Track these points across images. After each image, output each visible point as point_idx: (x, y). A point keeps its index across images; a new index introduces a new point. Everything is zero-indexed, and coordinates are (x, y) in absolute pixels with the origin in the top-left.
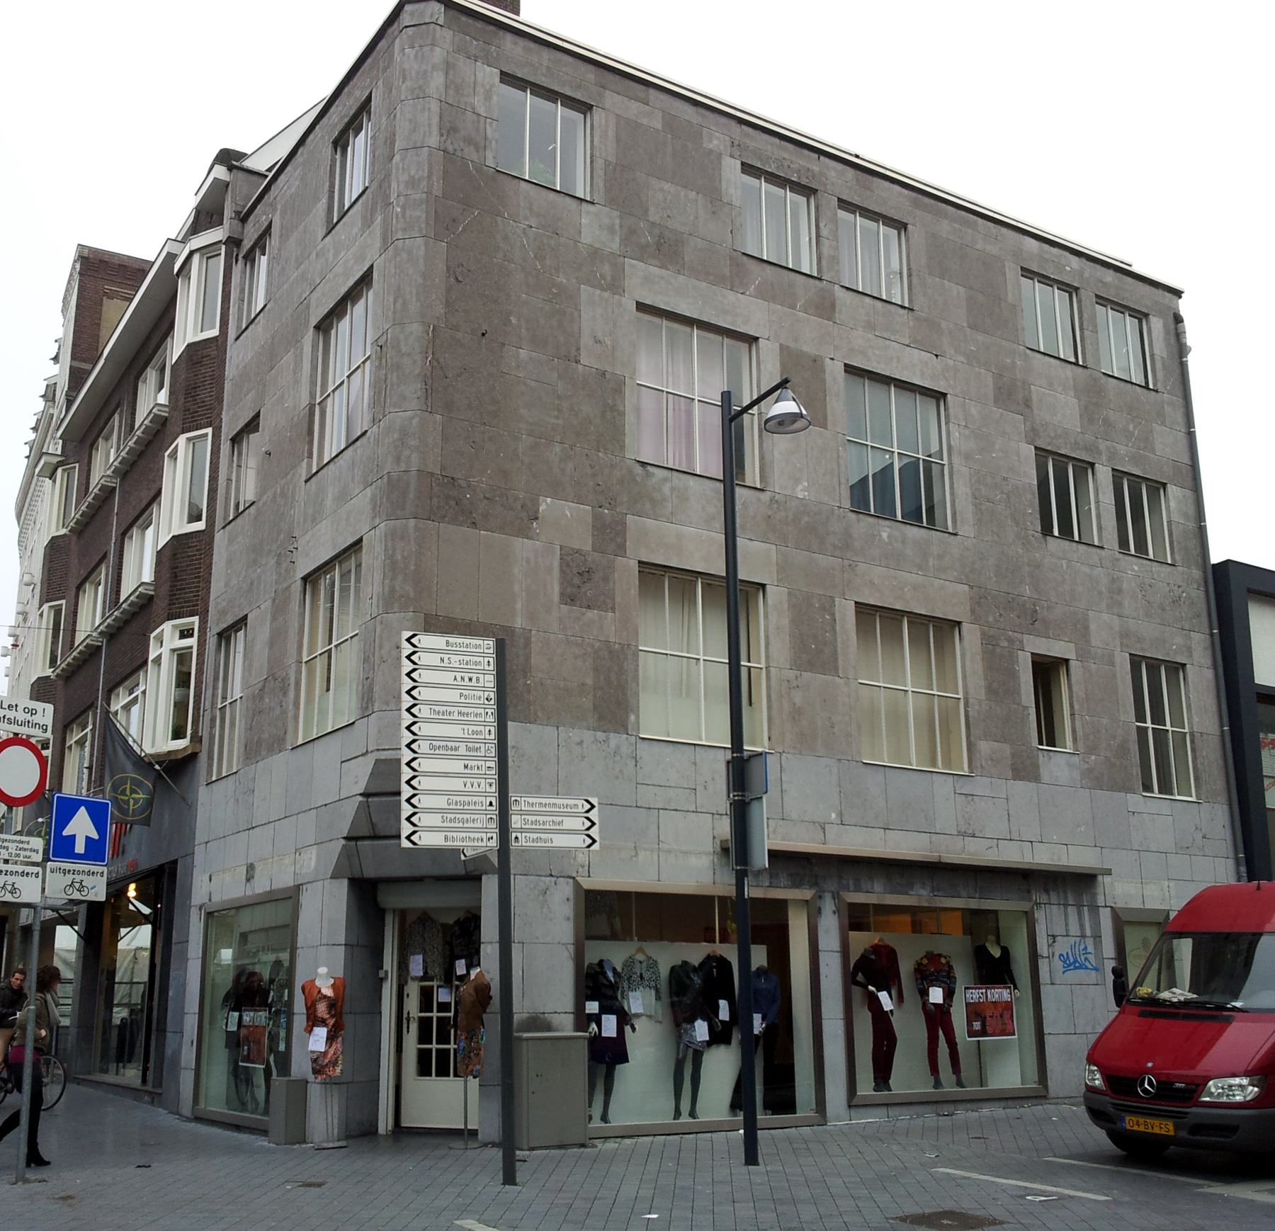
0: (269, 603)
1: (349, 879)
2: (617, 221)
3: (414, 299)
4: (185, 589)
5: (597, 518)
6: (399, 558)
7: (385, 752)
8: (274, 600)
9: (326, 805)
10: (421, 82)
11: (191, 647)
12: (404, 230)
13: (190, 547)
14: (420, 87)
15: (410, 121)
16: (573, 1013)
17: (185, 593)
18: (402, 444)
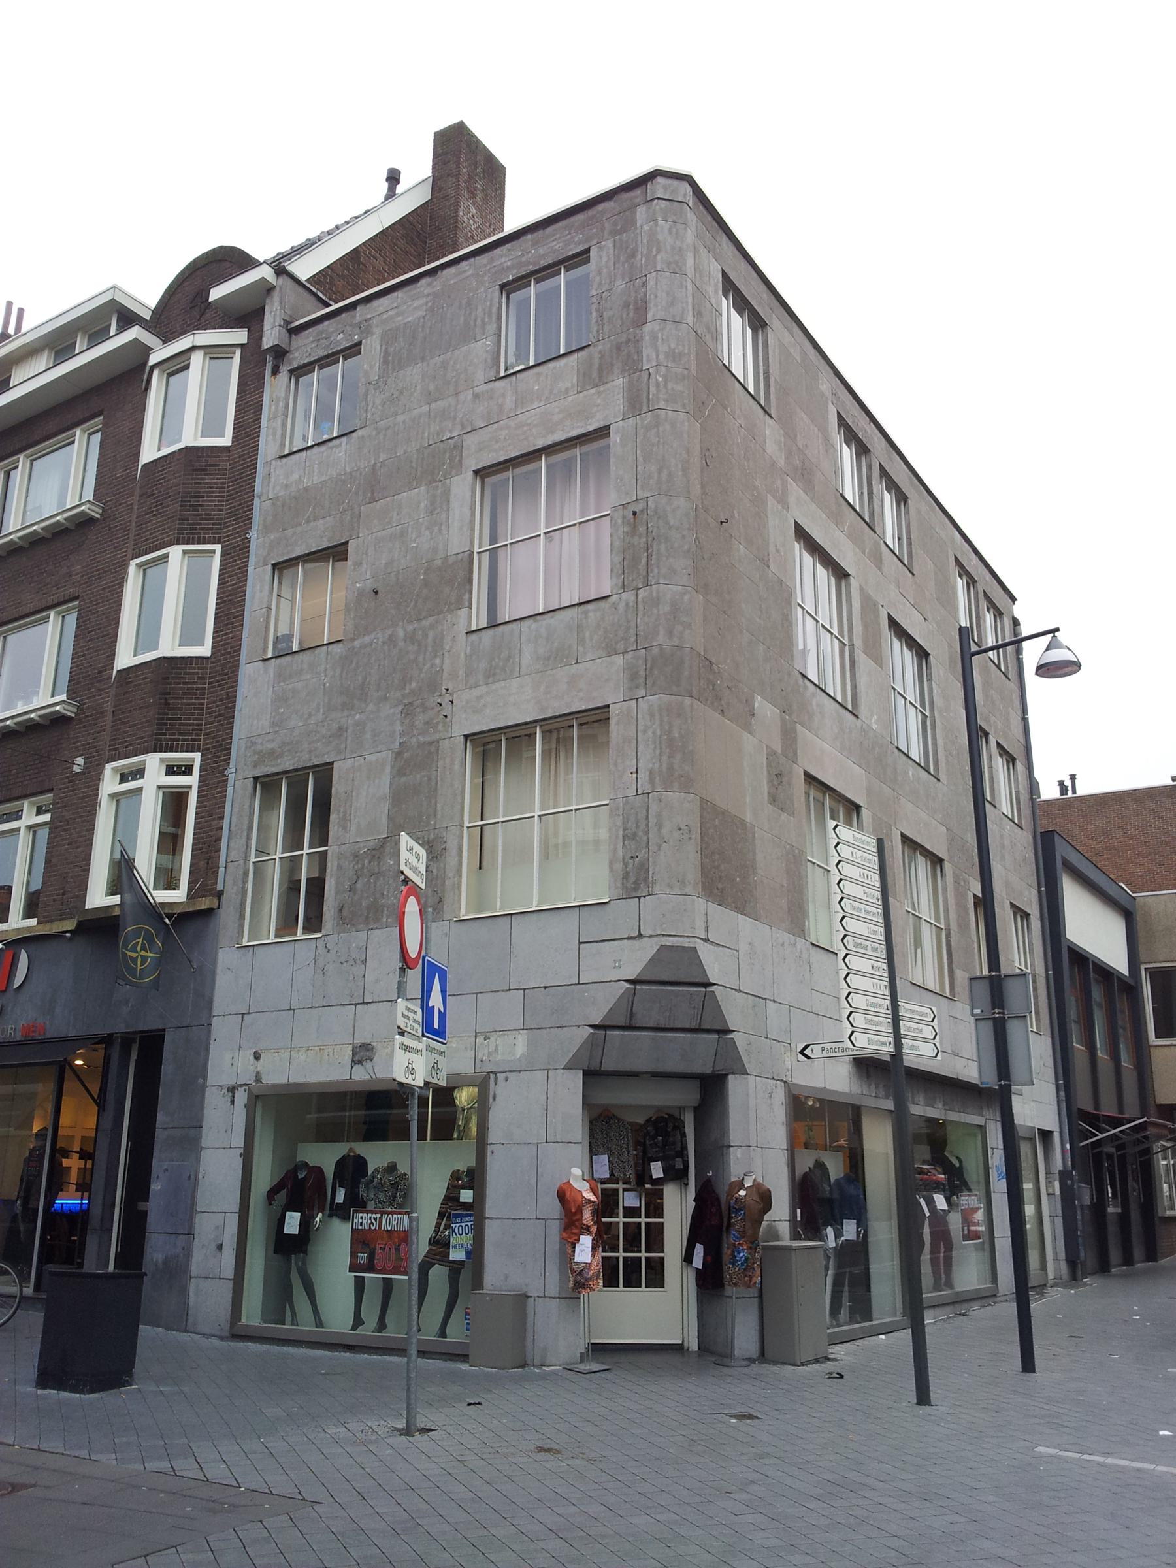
0: (388, 755)
1: (583, 1070)
2: (783, 440)
3: (680, 473)
4: (180, 719)
5: (783, 721)
6: (676, 735)
7: (671, 939)
8: (398, 754)
9: (545, 988)
10: (677, 258)
11: (190, 787)
12: (666, 401)
13: (186, 673)
14: (676, 263)
15: (668, 294)
16: (789, 1221)
17: (181, 724)
18: (674, 617)
